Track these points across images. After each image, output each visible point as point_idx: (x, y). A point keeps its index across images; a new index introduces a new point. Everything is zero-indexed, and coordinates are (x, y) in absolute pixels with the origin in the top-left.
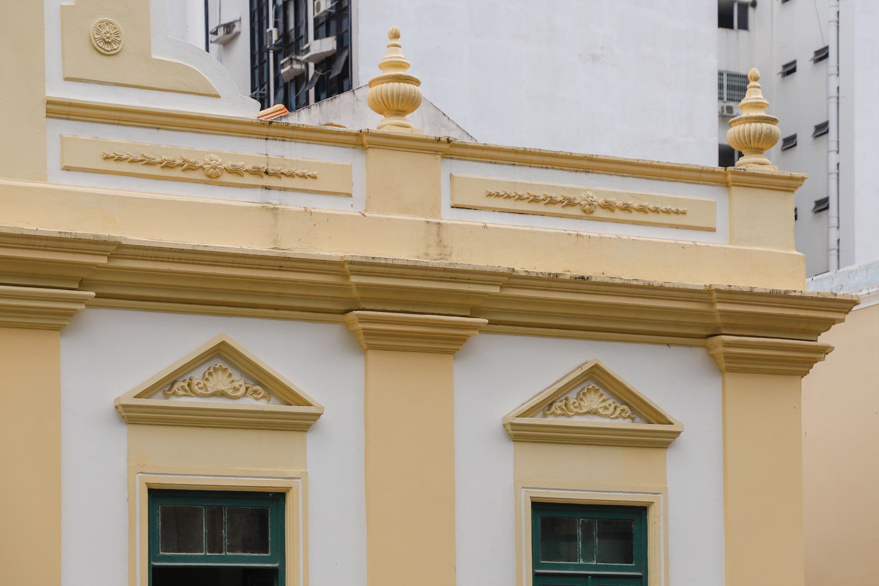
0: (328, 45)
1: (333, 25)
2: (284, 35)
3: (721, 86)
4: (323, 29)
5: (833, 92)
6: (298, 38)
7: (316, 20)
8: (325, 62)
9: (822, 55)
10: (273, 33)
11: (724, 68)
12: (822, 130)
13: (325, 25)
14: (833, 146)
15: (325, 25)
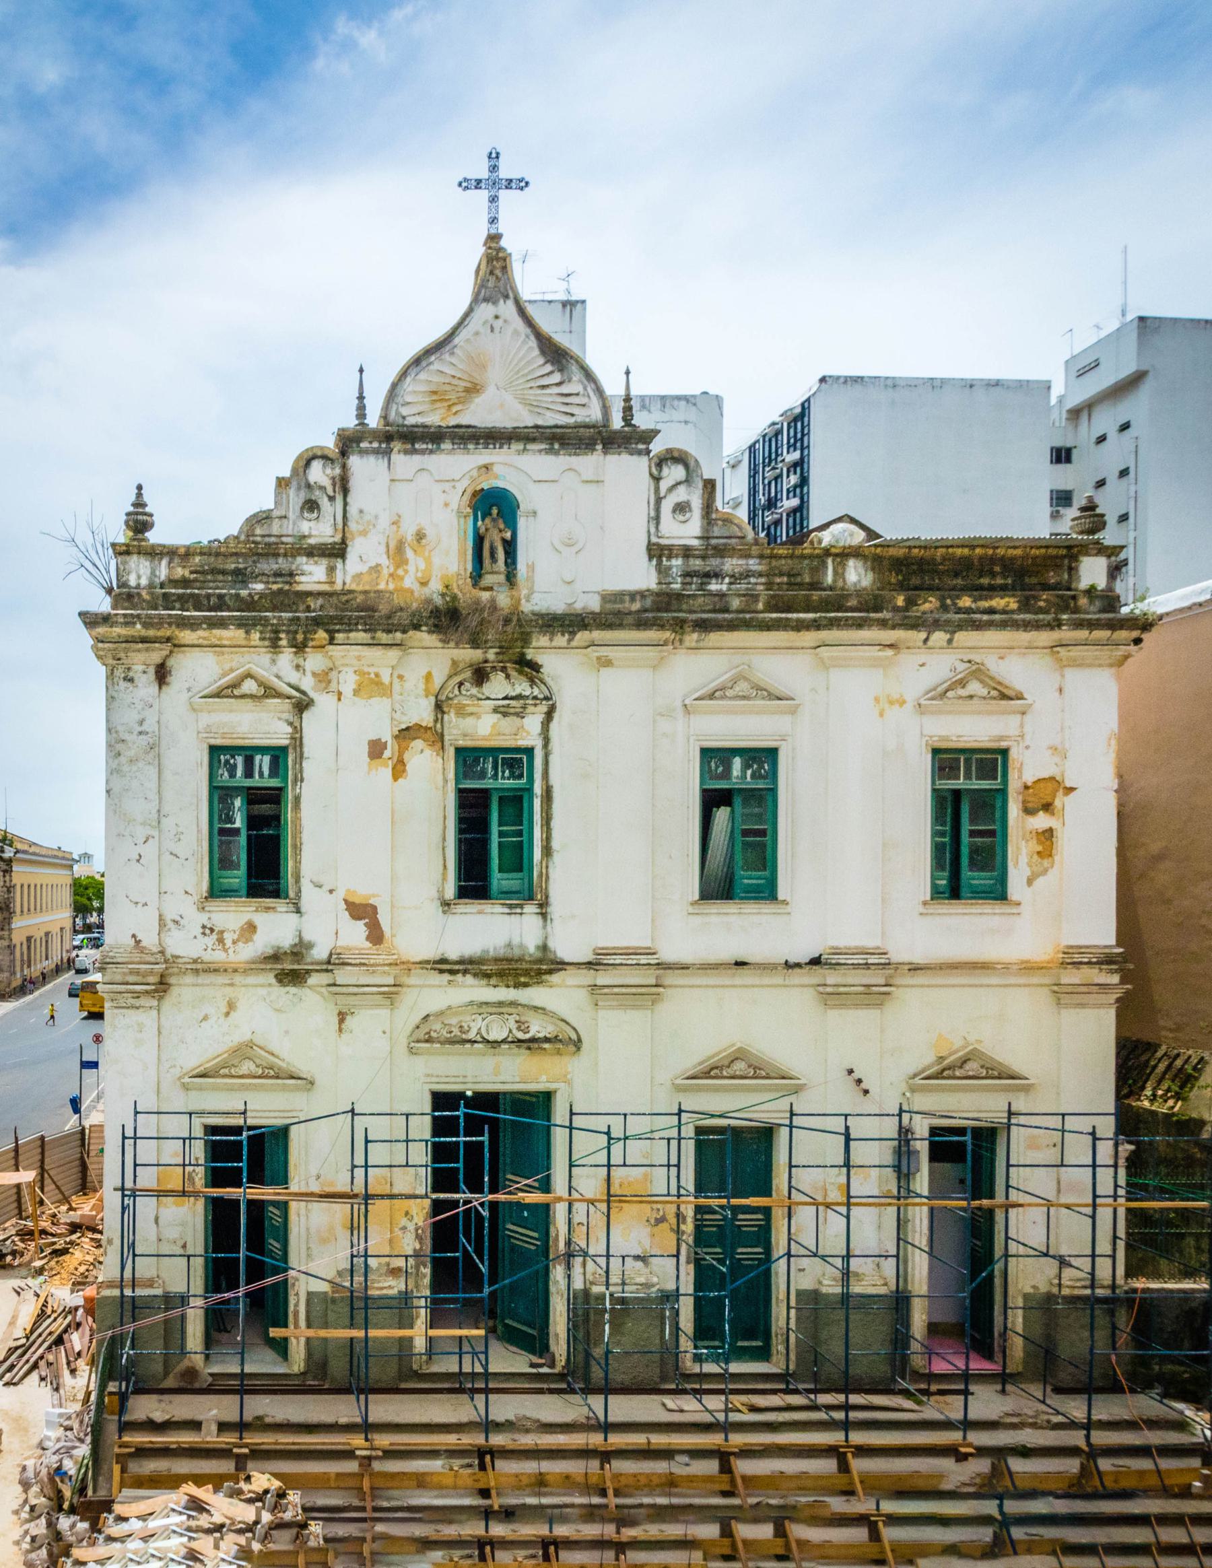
0: (795, 502)
1: (798, 491)
2: (769, 500)
3: (1052, 499)
4: (791, 494)
5: (1133, 494)
6: (776, 500)
7: (788, 490)
8: (795, 511)
9: (1124, 473)
10: (762, 499)
11: (1054, 488)
12: (1124, 518)
13: (792, 491)
14: (1132, 527)
15: (792, 491)
